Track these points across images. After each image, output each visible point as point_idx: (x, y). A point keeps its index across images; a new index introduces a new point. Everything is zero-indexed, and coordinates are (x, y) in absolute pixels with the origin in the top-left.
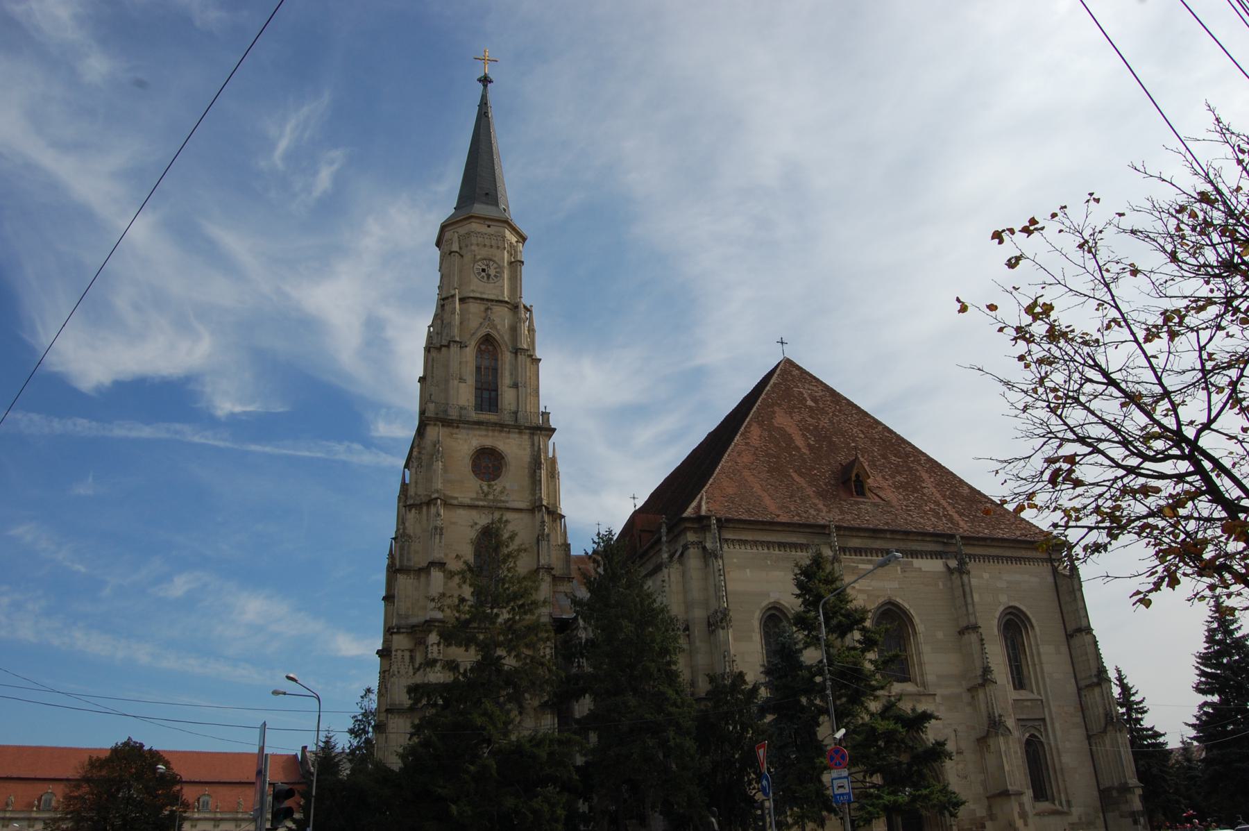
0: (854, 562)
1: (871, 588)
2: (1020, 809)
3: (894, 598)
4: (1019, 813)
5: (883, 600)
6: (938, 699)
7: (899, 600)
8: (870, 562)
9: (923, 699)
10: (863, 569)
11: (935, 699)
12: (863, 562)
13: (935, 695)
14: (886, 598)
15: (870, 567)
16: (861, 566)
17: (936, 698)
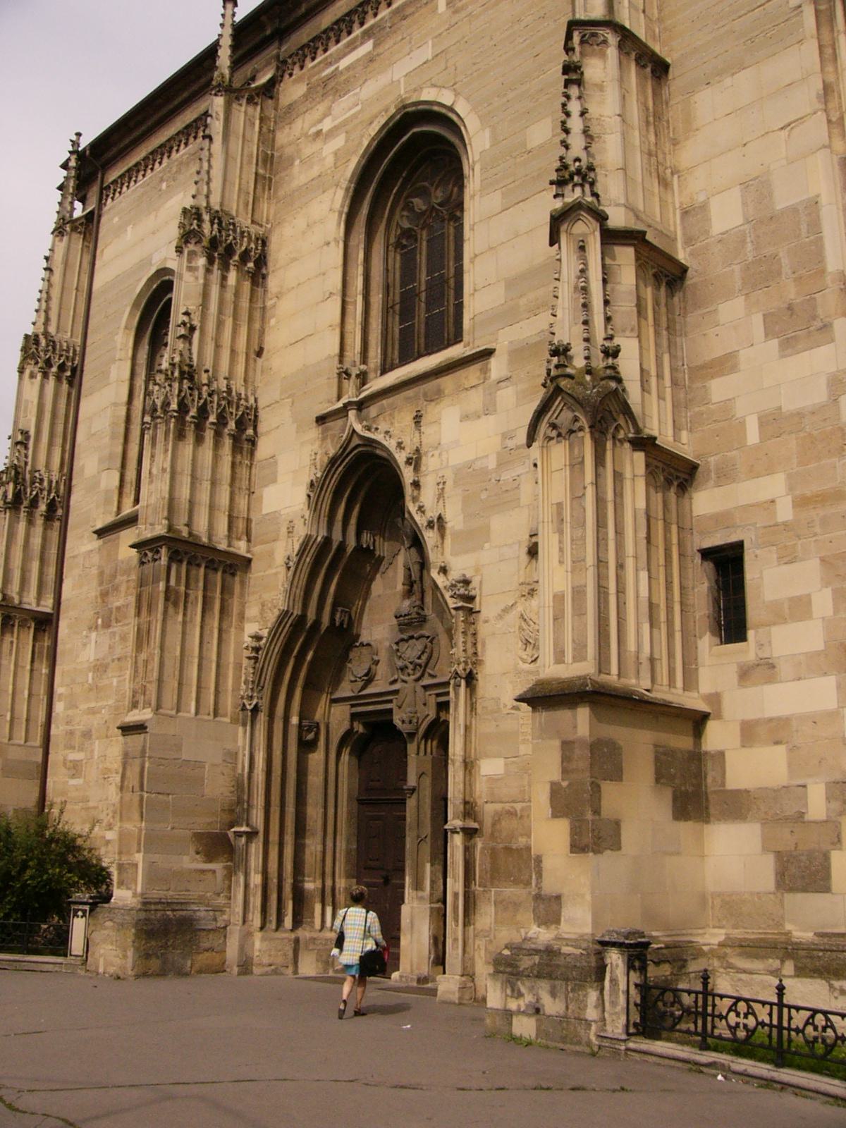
0: (331, 64)
1: (359, 108)
2: (565, 771)
3: (414, 99)
4: (553, 784)
5: (383, 121)
6: (497, 366)
7: (428, 95)
8: (367, 35)
9: (447, 382)
10: (348, 68)
11: (485, 371)
12: (352, 47)
13: (487, 354)
14: (393, 110)
15: (368, 46)
16: (343, 64)
17: (493, 362)
